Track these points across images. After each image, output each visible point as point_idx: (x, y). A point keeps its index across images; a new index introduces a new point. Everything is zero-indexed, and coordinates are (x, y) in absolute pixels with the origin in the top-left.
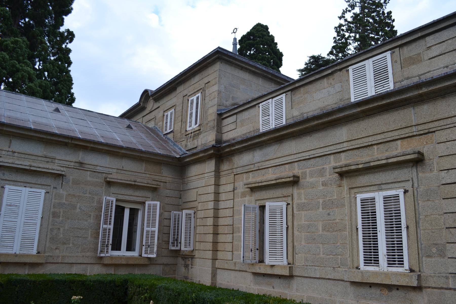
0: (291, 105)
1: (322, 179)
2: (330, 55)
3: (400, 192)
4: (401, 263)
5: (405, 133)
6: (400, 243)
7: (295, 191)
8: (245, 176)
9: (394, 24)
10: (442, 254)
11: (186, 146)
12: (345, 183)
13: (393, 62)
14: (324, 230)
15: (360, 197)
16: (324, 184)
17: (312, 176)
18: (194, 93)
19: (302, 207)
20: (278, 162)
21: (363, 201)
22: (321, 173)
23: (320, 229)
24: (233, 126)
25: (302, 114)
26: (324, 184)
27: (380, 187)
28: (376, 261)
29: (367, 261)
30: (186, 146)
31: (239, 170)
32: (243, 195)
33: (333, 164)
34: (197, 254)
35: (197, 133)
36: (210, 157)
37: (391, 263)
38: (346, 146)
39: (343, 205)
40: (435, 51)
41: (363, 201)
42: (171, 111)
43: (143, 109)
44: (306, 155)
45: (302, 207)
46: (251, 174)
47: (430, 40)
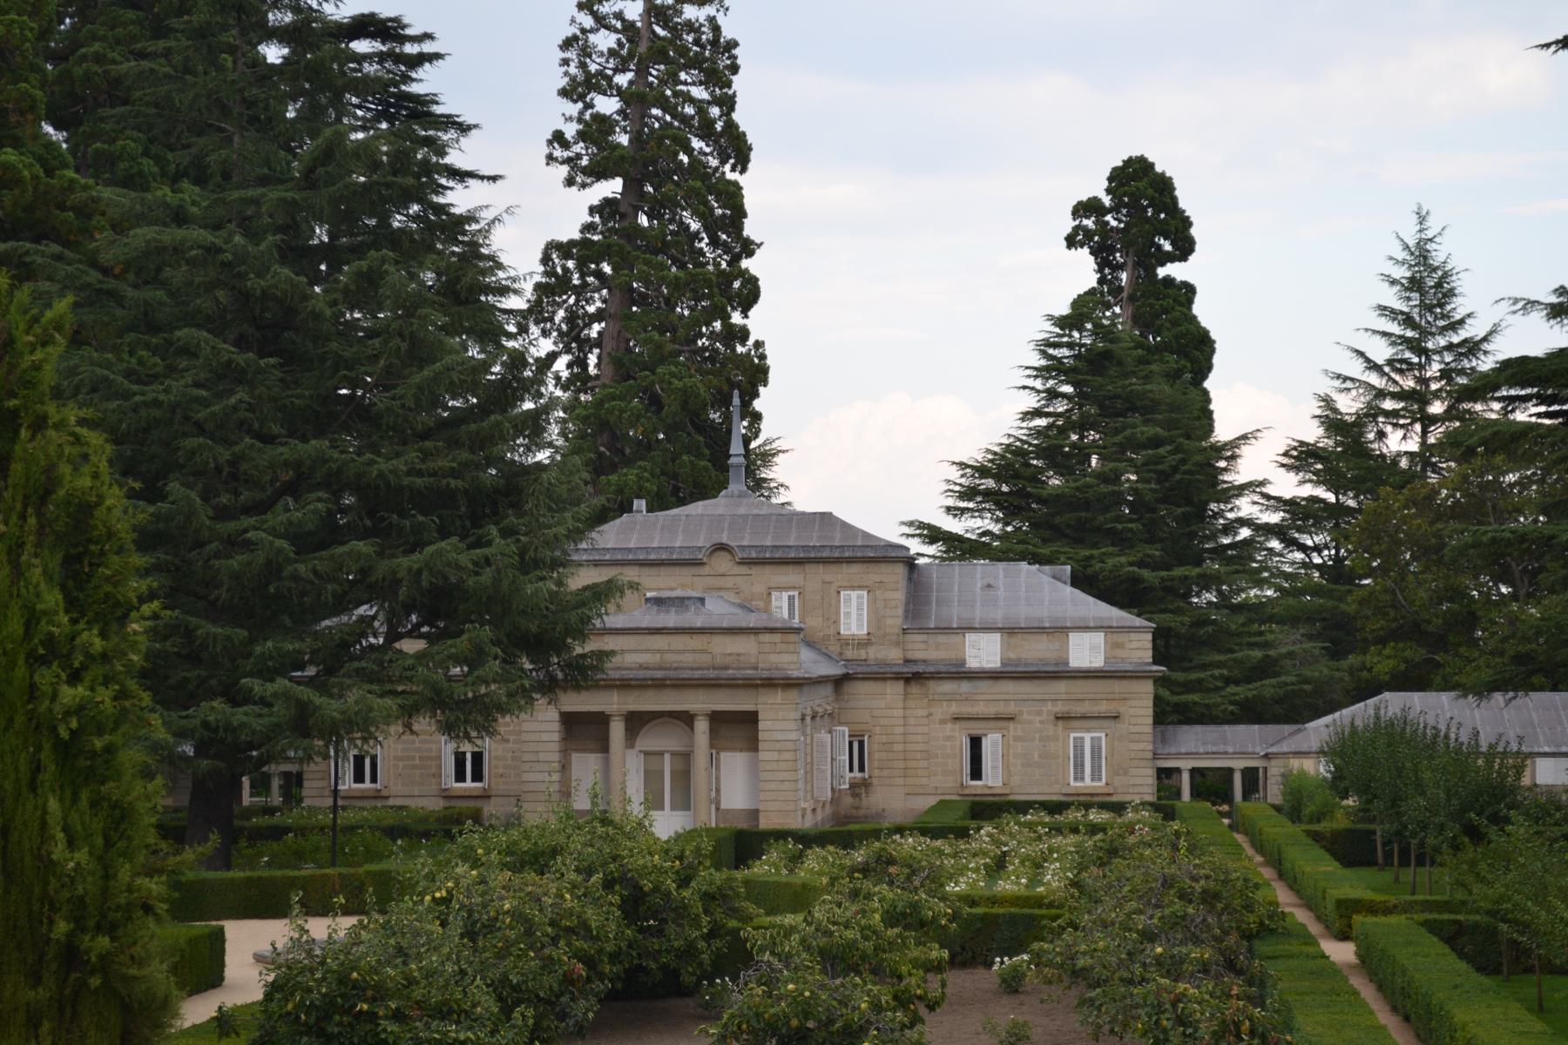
0: (1006, 647)
1: (1038, 718)
2: (556, 145)
3: (1103, 735)
4: (1100, 780)
5: (1109, 696)
6: (1100, 767)
7: (1011, 725)
8: (945, 703)
9: (734, 78)
10: (1126, 773)
11: (841, 654)
12: (1060, 723)
13: (1106, 642)
14: (1040, 756)
15: (1072, 735)
16: (1041, 722)
17: (1029, 713)
18: (853, 588)
19: (1016, 739)
20: (992, 697)
21: (1075, 738)
22: (1039, 713)
23: (1036, 756)
24: (922, 646)
25: (1020, 659)
26: (1041, 722)
27: (1088, 730)
28: (1083, 779)
29: (1076, 779)
30: (841, 654)
31: (936, 697)
32: (943, 722)
33: (1050, 707)
34: (875, 781)
35: (865, 643)
36: (897, 679)
37: (1092, 780)
38: (1064, 696)
39: (1058, 740)
40: (1134, 645)
41: (1075, 738)
42: (791, 593)
43: (703, 564)
44: (1025, 697)
45: (1016, 739)
46: (954, 703)
47: (1133, 636)
